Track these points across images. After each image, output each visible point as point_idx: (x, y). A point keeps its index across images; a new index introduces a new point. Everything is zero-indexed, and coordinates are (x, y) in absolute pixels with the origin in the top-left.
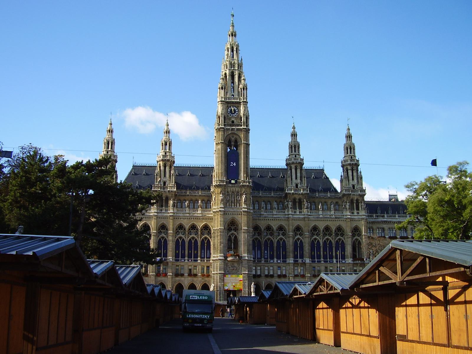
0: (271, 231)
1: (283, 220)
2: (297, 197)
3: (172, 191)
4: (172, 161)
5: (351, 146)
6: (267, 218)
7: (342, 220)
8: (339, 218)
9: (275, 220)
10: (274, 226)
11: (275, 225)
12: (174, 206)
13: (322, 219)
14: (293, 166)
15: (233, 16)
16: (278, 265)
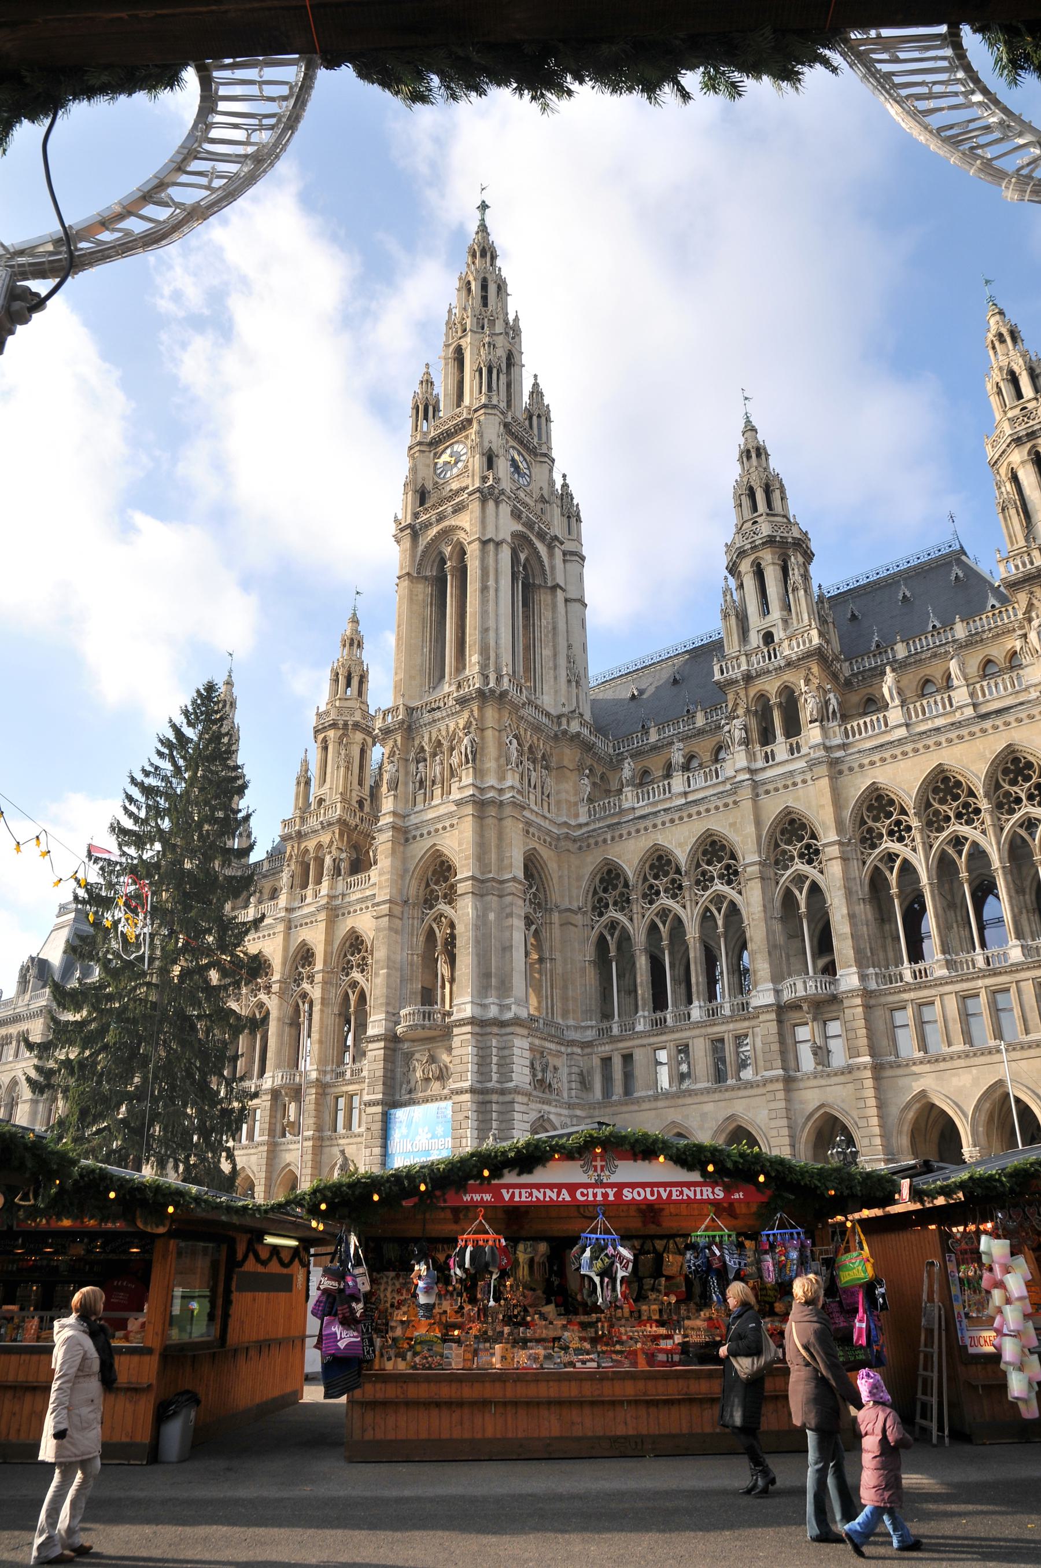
0: (671, 876)
1: (717, 808)
2: (771, 686)
3: (330, 824)
4: (346, 725)
5: (1016, 368)
6: (649, 823)
7: (1023, 715)
8: (999, 712)
9: (681, 818)
10: (680, 845)
11: (680, 842)
12: (337, 871)
13: (908, 748)
14: (745, 566)
15: (484, 207)
16: (710, 1030)
